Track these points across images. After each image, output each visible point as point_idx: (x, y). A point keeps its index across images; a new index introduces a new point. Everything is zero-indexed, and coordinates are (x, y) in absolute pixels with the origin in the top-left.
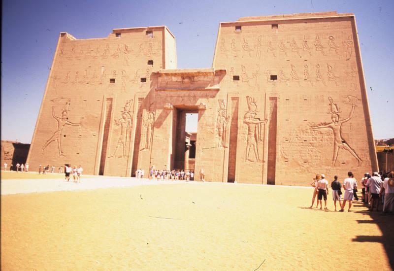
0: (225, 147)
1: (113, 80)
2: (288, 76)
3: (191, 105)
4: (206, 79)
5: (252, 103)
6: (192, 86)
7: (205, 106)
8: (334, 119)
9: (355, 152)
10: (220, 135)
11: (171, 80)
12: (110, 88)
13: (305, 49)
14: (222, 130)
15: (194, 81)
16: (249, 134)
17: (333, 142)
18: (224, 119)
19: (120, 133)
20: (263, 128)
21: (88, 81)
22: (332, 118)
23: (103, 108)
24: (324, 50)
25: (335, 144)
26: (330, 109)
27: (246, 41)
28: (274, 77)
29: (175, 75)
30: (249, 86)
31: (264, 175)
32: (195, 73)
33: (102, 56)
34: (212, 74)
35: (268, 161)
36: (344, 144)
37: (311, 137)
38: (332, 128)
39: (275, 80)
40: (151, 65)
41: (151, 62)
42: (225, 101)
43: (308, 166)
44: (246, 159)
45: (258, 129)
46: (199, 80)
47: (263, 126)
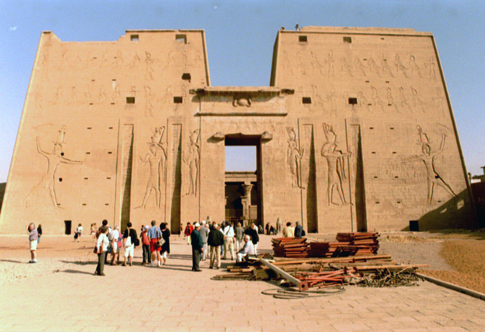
0: (301, 187)
1: (131, 100)
2: (370, 101)
5: (329, 132)
6: (249, 111)
7: (272, 135)
9: (450, 189)
10: (293, 173)
14: (295, 166)
16: (329, 170)
17: (426, 178)
18: (296, 153)
19: (149, 173)
22: (423, 149)
23: (120, 138)
25: (428, 179)
26: (419, 139)
27: (314, 55)
28: (353, 101)
30: (324, 110)
31: (353, 220)
35: (356, 203)
36: (439, 179)
38: (424, 161)
39: (355, 105)
40: (187, 81)
41: (187, 77)
42: (296, 130)
45: (341, 165)
47: (346, 160)
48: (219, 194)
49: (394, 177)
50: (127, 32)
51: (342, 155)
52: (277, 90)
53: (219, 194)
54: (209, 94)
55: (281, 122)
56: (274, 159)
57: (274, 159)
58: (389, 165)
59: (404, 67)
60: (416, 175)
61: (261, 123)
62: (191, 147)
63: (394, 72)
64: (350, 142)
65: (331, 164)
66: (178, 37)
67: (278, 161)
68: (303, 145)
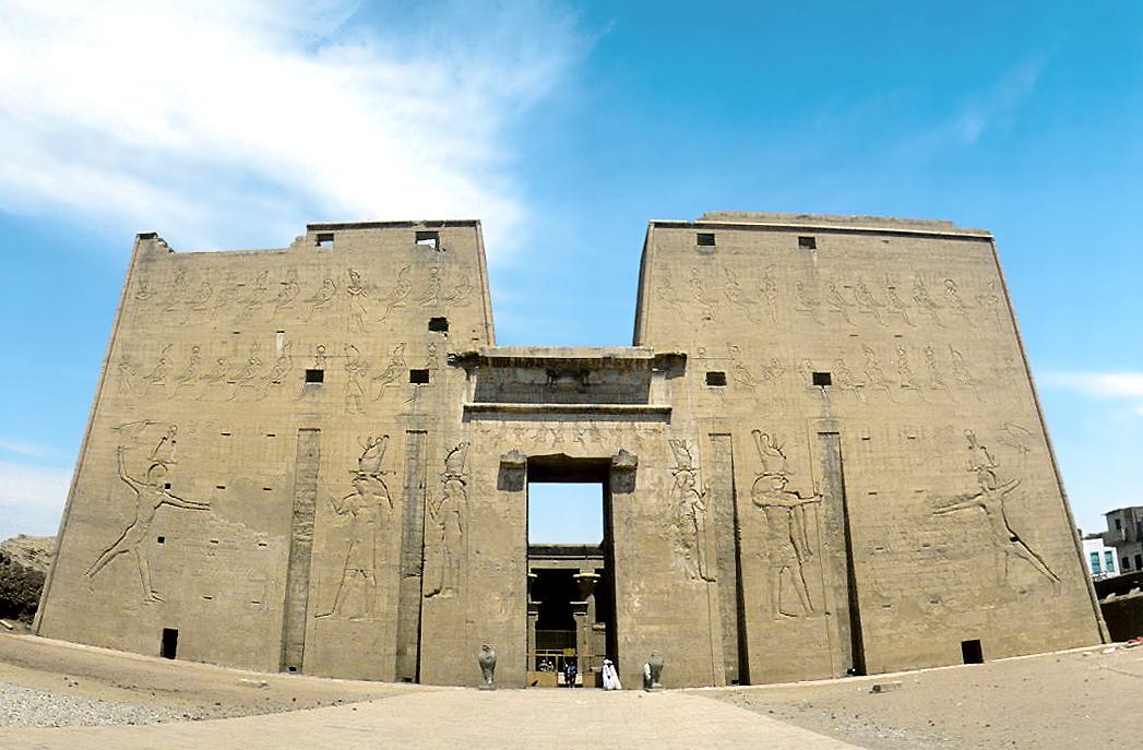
1: (315, 376)
2: (860, 376)
3: (585, 455)
4: (626, 379)
7: (636, 458)
8: (985, 484)
11: (511, 379)
12: (307, 399)
13: (892, 308)
14: (692, 529)
20: (811, 520)
21: (235, 373)
24: (939, 312)
28: (822, 379)
29: (529, 363)
33: (274, 300)
37: (938, 533)
41: (439, 325)
43: (942, 611)
44: (774, 609)
48: (512, 594)
49: (920, 543)
50: (310, 228)
51: (801, 501)
52: (647, 356)
56: (641, 511)
58: (909, 520)
59: (933, 305)
60: (969, 539)
61: (611, 431)
63: (912, 314)
64: (819, 472)
65: (776, 522)
66: (421, 236)
67: (650, 518)
68: (708, 480)
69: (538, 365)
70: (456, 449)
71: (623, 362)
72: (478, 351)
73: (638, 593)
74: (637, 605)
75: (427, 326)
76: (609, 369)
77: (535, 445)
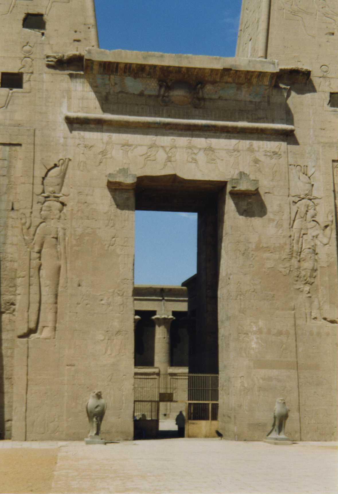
4: (244, 95)
7: (256, 181)
11: (118, 89)
15: (204, 99)
32: (212, 70)
34: (266, 81)
41: (34, 21)
46: (220, 98)
48: (118, 332)
53: (118, 332)
54: (96, 67)
55: (277, 150)
56: (260, 241)
57: (260, 241)
61: (228, 151)
62: (46, 204)
67: (267, 249)
69: (149, 74)
70: (56, 166)
71: (243, 76)
72: (83, 53)
73: (255, 333)
74: (254, 346)
75: (21, 22)
76: (226, 83)
77: (145, 165)
